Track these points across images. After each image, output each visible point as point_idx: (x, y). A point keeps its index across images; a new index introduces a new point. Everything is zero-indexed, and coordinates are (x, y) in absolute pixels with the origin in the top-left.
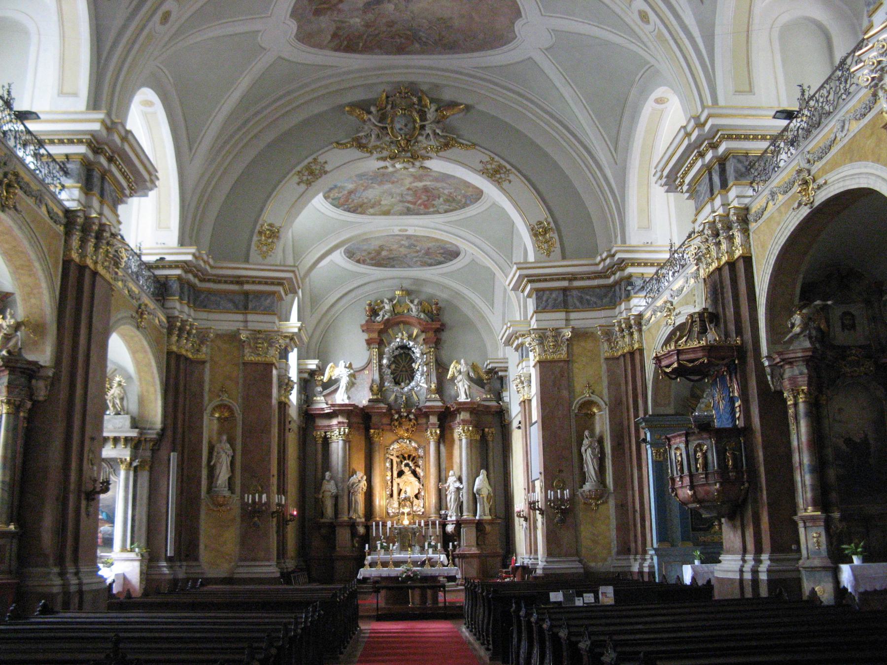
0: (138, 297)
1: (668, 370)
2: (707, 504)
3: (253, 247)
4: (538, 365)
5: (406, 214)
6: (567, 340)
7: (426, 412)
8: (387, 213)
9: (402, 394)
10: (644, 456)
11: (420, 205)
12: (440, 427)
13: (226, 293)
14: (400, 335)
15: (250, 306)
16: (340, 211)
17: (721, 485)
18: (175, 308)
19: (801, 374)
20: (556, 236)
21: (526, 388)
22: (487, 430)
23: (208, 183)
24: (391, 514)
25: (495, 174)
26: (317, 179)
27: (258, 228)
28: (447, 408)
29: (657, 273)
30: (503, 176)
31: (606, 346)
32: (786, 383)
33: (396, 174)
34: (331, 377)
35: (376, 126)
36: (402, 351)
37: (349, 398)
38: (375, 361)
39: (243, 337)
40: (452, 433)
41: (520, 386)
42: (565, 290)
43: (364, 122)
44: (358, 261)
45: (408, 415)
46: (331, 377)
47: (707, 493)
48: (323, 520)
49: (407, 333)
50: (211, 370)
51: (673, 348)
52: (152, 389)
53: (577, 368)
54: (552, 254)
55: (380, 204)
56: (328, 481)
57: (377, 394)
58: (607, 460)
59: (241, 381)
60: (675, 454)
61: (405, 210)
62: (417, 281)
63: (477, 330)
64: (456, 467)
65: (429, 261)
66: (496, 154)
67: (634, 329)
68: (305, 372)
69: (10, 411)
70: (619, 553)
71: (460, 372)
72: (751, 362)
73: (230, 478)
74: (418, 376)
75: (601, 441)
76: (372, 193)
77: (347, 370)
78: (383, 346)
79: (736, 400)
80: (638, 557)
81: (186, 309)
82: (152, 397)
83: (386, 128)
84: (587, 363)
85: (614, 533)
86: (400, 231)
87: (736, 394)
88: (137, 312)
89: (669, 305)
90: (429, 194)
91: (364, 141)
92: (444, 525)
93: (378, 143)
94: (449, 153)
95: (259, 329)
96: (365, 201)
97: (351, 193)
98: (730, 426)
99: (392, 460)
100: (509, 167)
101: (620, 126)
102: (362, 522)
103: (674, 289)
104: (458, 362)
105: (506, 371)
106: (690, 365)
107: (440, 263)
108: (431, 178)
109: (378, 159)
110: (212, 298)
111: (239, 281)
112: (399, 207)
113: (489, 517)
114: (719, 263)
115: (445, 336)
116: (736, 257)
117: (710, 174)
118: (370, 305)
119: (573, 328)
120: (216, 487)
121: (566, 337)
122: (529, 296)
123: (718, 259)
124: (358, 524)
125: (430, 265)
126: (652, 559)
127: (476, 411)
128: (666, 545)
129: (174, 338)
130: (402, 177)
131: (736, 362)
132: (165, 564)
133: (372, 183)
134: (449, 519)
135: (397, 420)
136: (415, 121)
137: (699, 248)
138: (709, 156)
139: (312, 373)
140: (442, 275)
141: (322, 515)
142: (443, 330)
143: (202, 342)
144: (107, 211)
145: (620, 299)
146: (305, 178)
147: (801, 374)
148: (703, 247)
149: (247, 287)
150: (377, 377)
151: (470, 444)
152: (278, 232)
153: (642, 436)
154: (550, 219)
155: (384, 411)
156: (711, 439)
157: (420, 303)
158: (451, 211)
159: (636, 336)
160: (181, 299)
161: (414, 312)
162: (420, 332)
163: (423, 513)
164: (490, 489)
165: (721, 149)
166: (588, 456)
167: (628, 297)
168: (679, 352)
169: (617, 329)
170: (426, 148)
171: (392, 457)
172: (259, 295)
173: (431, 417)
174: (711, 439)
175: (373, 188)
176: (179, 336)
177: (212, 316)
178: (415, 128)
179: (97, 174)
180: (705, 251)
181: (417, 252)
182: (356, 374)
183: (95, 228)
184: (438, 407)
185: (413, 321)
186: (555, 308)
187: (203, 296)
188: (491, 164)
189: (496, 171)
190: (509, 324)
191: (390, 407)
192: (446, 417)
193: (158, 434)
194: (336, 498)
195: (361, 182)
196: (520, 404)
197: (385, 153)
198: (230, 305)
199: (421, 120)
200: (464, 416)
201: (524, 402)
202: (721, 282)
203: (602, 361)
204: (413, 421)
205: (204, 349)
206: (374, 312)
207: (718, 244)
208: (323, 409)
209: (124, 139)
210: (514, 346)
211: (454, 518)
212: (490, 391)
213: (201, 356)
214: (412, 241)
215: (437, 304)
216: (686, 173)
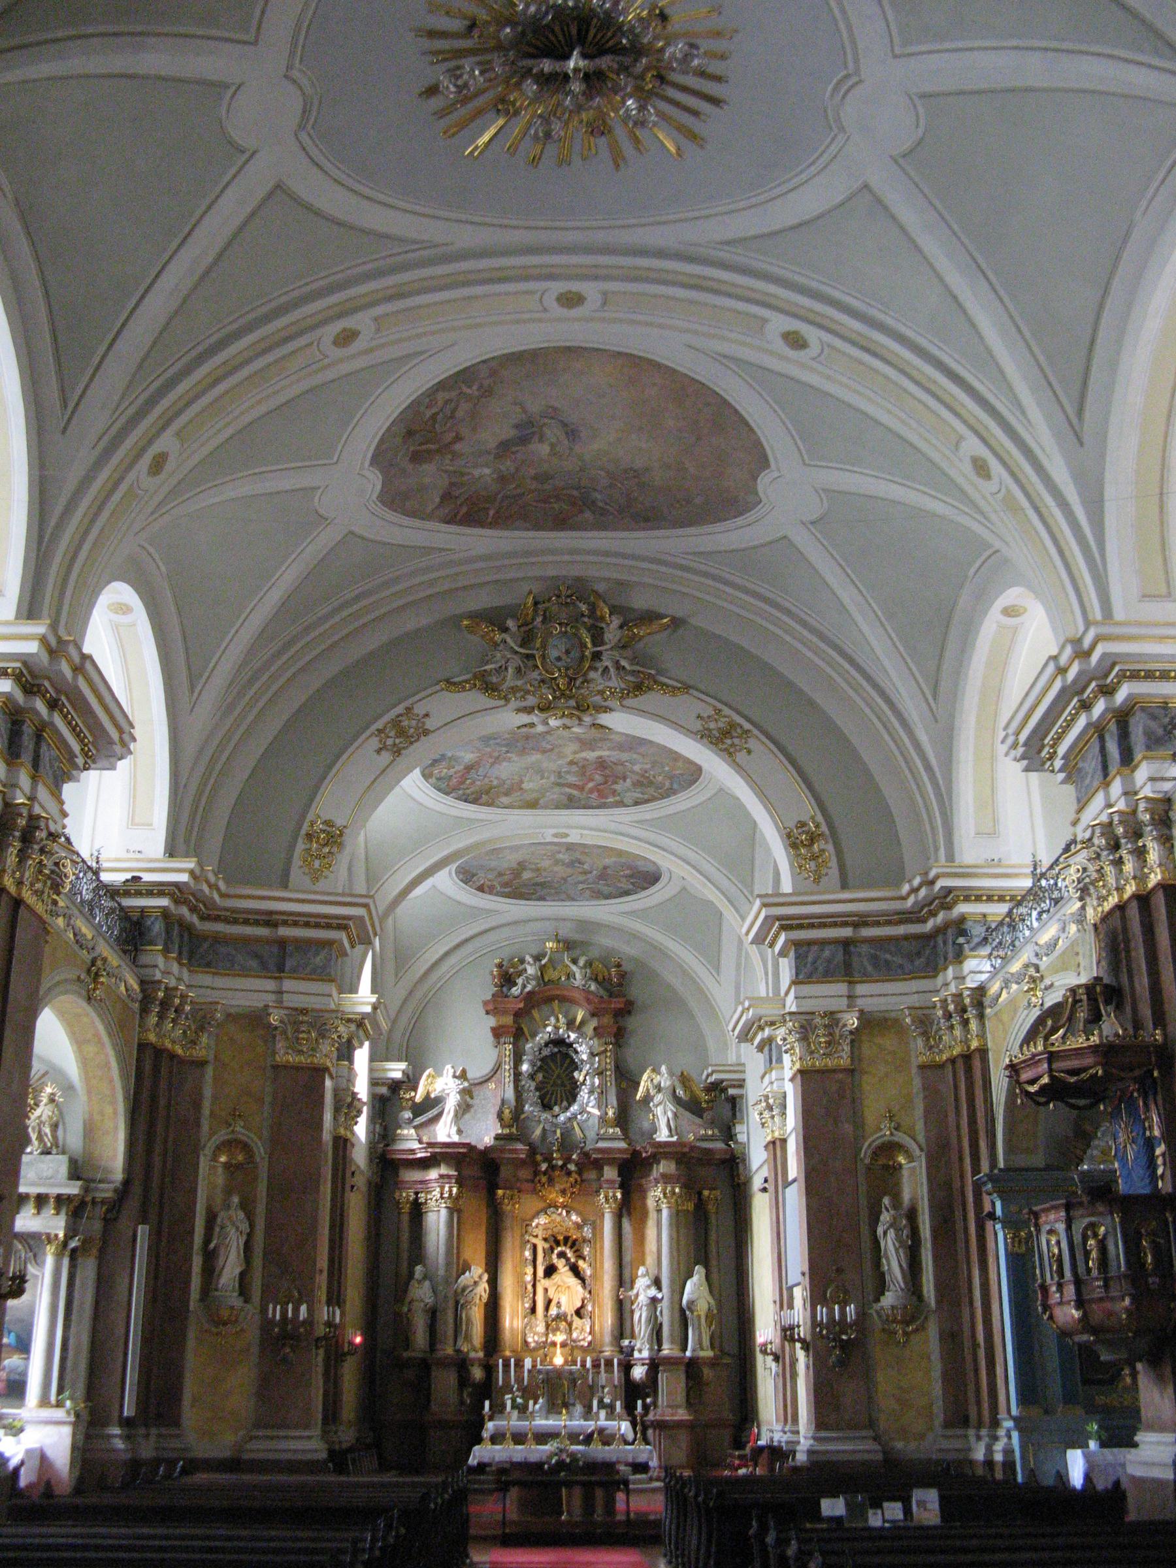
0: (90, 945)
1: (1032, 1089)
2: (1109, 1336)
3: (297, 861)
4: (799, 1076)
5: (567, 807)
6: (851, 1032)
7: (596, 1160)
8: (533, 805)
9: (556, 1126)
10: (990, 1245)
11: (591, 791)
12: (622, 1186)
13: (247, 940)
14: (553, 1020)
15: (289, 963)
16: (449, 800)
17: (1134, 1299)
18: (156, 966)
20: (830, 847)
21: (777, 1119)
22: (706, 1193)
23: (221, 746)
24: (533, 1345)
26: (411, 743)
27: (306, 827)
28: (635, 1154)
29: (1010, 914)
30: (736, 741)
31: (920, 1042)
33: (548, 737)
34: (428, 1093)
35: (516, 652)
36: (556, 1050)
37: (459, 1132)
39: (274, 1020)
40: (644, 1198)
41: (766, 1114)
42: (846, 943)
43: (496, 645)
44: (481, 889)
45: (564, 1165)
46: (428, 1093)
47: (1110, 1314)
48: (405, 1354)
49: (565, 1016)
50: (216, 1079)
51: (1040, 1048)
52: (109, 1110)
53: (868, 1083)
54: (824, 880)
56: (419, 1282)
57: (510, 1126)
58: (923, 1251)
59: (268, 1099)
60: (1048, 1242)
61: (564, 799)
62: (584, 925)
63: (691, 1016)
64: (650, 1259)
65: (606, 890)
67: (971, 1013)
68: (383, 1084)
70: (947, 1424)
71: (659, 1088)
73: (242, 1275)
74: (584, 1094)
75: (912, 1215)
76: (506, 771)
77: (458, 1082)
78: (522, 1040)
79: (1156, 1142)
80: (984, 1432)
81: (175, 968)
82: (109, 1124)
83: (533, 656)
84: (887, 1075)
85: (937, 1389)
86: (555, 835)
87: (1157, 1133)
88: (89, 971)
89: (1032, 971)
91: (494, 680)
92: (627, 1367)
93: (519, 683)
95: (300, 1005)
96: (495, 783)
97: (469, 768)
98: (1147, 1191)
99: (535, 1247)
100: (747, 726)
101: (941, 656)
102: (479, 1359)
103: (1042, 942)
104: (656, 1070)
106: (1073, 1080)
107: (627, 893)
109: (519, 710)
110: (223, 950)
111: (270, 920)
112: (555, 795)
114: (1121, 896)
115: (632, 1023)
116: (1150, 885)
117: (1102, 739)
118: (500, 966)
119: (861, 1012)
120: (216, 1290)
121: (849, 1028)
122: (782, 954)
123: (1121, 889)
124: (472, 1362)
125: (607, 897)
126: (1009, 1437)
128: (1035, 1411)
129: (153, 1019)
131: (1156, 1074)
132: (117, 1431)
133: (507, 752)
134: (636, 1355)
135: (545, 1173)
136: (583, 646)
137: (1085, 870)
138: (1099, 707)
139: (395, 1086)
140: (632, 913)
141: (407, 1343)
142: (629, 1012)
143: (202, 1028)
144: (43, 793)
145: (946, 959)
146: (390, 742)
148: (1092, 868)
149: (283, 931)
150: (510, 1094)
151: (677, 1216)
152: (341, 835)
153: (987, 1208)
154: (820, 818)
155: (523, 1156)
156: (1112, 1214)
157: (589, 964)
158: (647, 801)
159: (974, 1025)
160: (166, 950)
161: (579, 979)
163: (590, 1343)
164: (712, 1302)
165: (1121, 696)
166: (889, 1243)
167: (959, 957)
168: (1052, 1057)
169: (940, 1013)
170: (602, 692)
171: (534, 1240)
172: (304, 946)
173: (606, 1168)
174: (1112, 1214)
175: (509, 760)
176: (161, 1016)
177: (220, 982)
178: (583, 657)
179: (28, 730)
180: (1095, 875)
181: (585, 873)
183: (22, 822)
184: (620, 1150)
185: (577, 995)
186: (828, 975)
187: (206, 945)
189: (726, 733)
190: (747, 1004)
191: (533, 1150)
193: (115, 1190)
194: (433, 1314)
195: (488, 750)
196: (766, 1147)
197: (531, 701)
198: (254, 963)
199: (594, 645)
200: (665, 1167)
201: (774, 1143)
202: (1125, 930)
203: (914, 1070)
205: (204, 1039)
206: (507, 979)
207: (1119, 862)
208: (413, 1151)
209: (78, 669)
210: (756, 1041)
211: (645, 1354)
212: (712, 1124)
213: (199, 1053)
214: (578, 855)
215: (619, 965)
216: (1059, 738)
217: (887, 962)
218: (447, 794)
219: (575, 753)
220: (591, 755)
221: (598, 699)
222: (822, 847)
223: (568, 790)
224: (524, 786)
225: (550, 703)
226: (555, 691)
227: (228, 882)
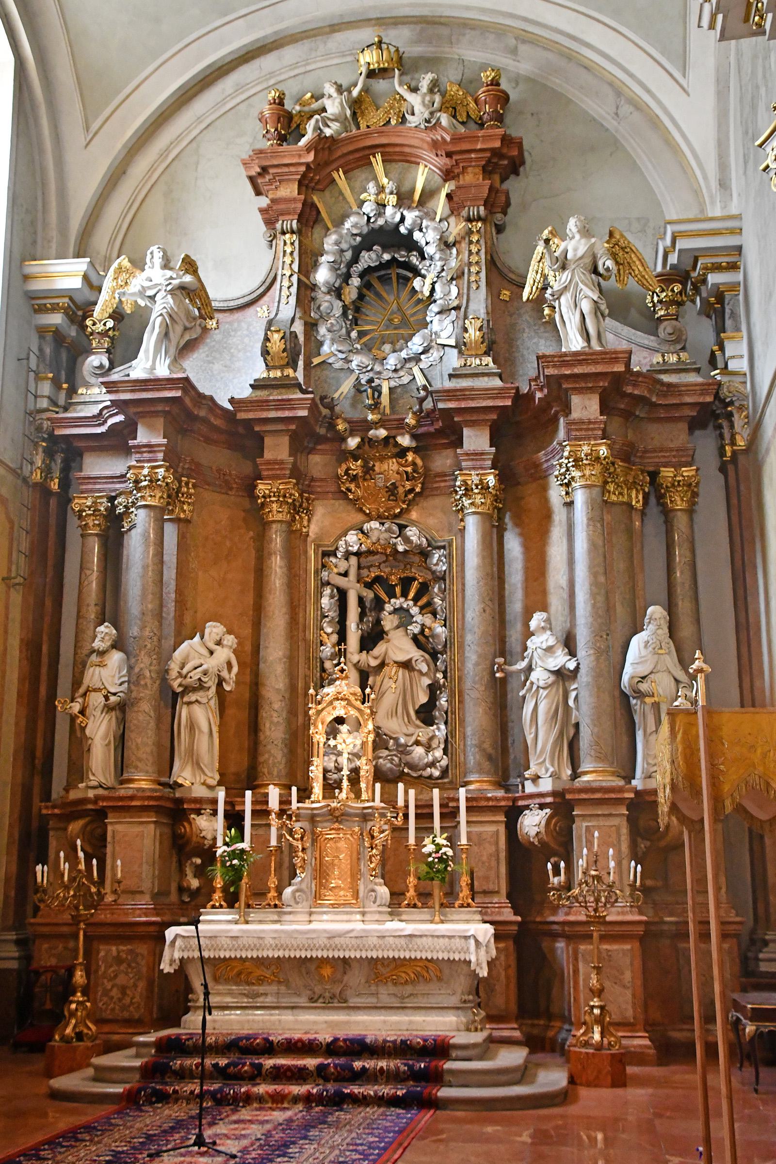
22: (667, 473)
36: (386, 257)
38: (289, 266)
56: (102, 653)
64: (556, 601)
68: (55, 308)
78: (318, 230)
92: (513, 814)
99: (342, 596)
105: (733, 267)
155: (304, 413)
162: (438, 179)
163: (445, 772)
171: (341, 582)
173: (467, 432)
184: (487, 393)
204: (410, 457)
211: (546, 785)
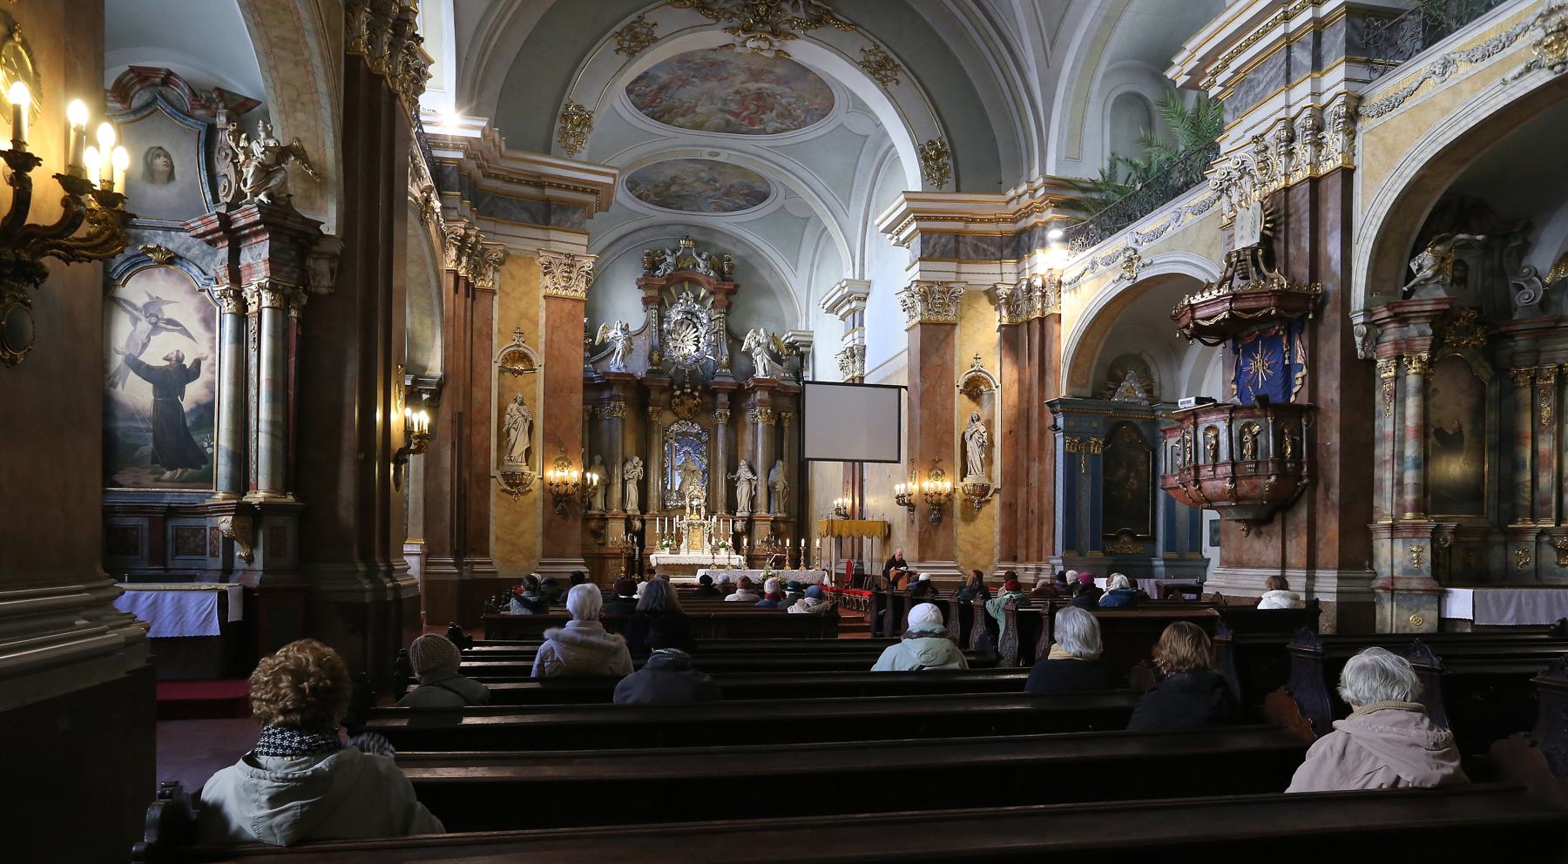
1: (1206, 323)
3: (556, 137)
8: (698, 126)
9: (684, 366)
13: (520, 198)
16: (641, 115)
18: (455, 208)
19: (1422, 334)
20: (950, 162)
22: (784, 414)
25: (879, 70)
26: (644, 48)
30: (889, 73)
32: (1387, 348)
42: (957, 235)
44: (640, 197)
45: (692, 392)
50: (501, 304)
54: (944, 186)
55: (694, 112)
66: (882, 42)
69: (277, 304)
71: (759, 344)
72: (1332, 316)
76: (686, 95)
78: (663, 308)
85: (997, 539)
86: (710, 154)
87: (1300, 361)
89: (1132, 252)
90: (761, 103)
94: (820, 32)
96: (677, 103)
97: (662, 88)
100: (897, 61)
104: (757, 332)
107: (741, 208)
108: (772, 77)
111: (539, 182)
112: (717, 120)
113: (784, 515)
125: (725, 211)
127: (774, 390)
128: (1073, 554)
130: (735, 71)
133: (694, 76)
146: (626, 44)
147: (1422, 334)
149: (549, 192)
152: (589, 119)
153: (1050, 422)
154: (945, 140)
155: (667, 385)
156: (1266, 416)
158: (783, 131)
162: (708, 294)
170: (790, 21)
173: (720, 395)
182: (633, 338)
184: (731, 384)
185: (701, 279)
186: (944, 257)
187: (487, 200)
188: (875, 54)
189: (881, 66)
191: (671, 384)
192: (738, 397)
195: (681, 72)
197: (736, 22)
198: (525, 216)
215: (729, 260)
217: (984, 250)
218: (640, 109)
219: (742, 83)
220: (753, 86)
221: (786, 27)
222: (945, 161)
223: (728, 116)
224: (698, 110)
225: (751, 25)
226: (755, 16)
227: (508, 147)
